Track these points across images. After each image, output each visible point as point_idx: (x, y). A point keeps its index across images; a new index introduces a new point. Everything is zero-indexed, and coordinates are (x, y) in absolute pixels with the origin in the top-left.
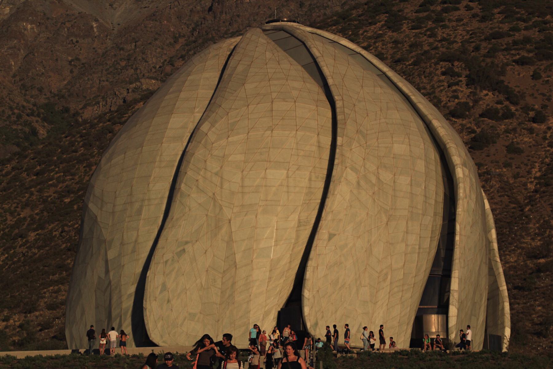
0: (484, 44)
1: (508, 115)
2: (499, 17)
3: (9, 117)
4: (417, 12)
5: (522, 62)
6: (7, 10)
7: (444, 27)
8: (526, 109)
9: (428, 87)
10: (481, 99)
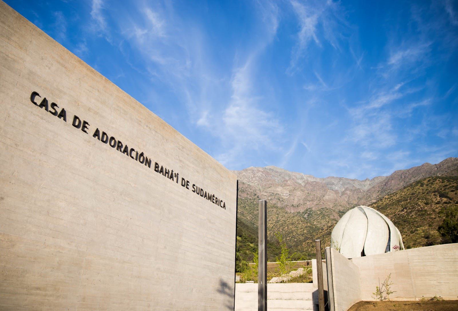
0: (443, 188)
1: (450, 203)
2: (446, 182)
3: (346, 210)
4: (427, 182)
5: (452, 191)
6: (344, 189)
7: (433, 185)
8: (454, 201)
9: (430, 198)
10: (443, 200)
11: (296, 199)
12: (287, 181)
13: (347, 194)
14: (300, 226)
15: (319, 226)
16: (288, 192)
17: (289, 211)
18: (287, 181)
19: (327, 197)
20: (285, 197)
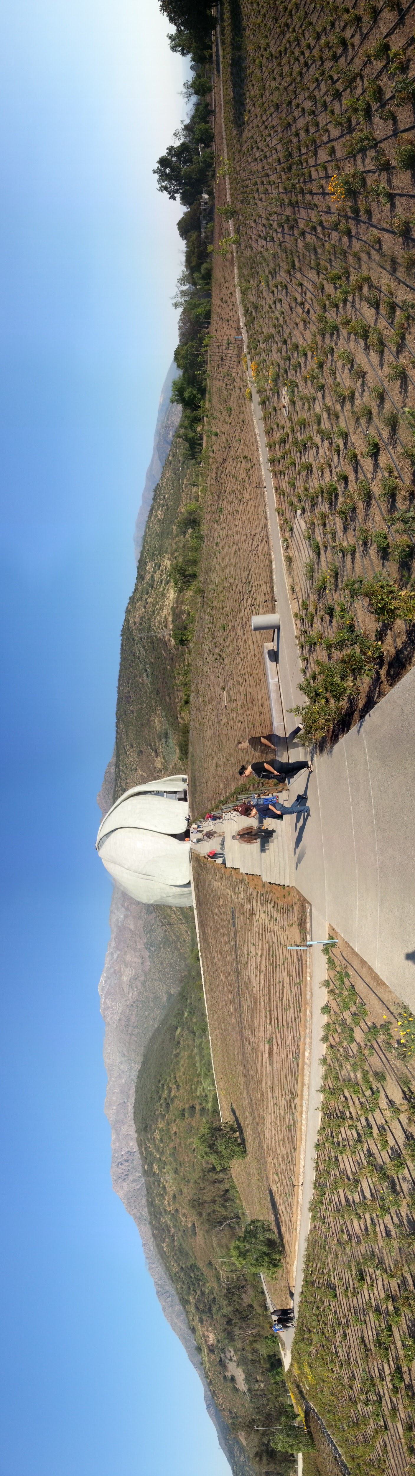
11: (135, 960)
12: (115, 970)
13: (128, 906)
14: (163, 956)
15: (162, 935)
16: (127, 969)
17: (149, 967)
18: (115, 970)
19: (132, 927)
20: (134, 972)
